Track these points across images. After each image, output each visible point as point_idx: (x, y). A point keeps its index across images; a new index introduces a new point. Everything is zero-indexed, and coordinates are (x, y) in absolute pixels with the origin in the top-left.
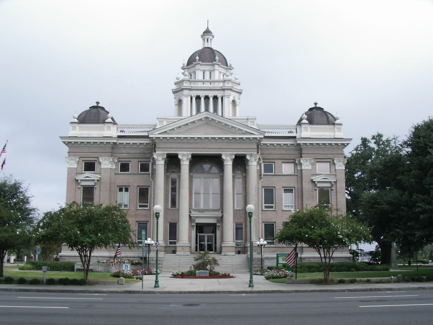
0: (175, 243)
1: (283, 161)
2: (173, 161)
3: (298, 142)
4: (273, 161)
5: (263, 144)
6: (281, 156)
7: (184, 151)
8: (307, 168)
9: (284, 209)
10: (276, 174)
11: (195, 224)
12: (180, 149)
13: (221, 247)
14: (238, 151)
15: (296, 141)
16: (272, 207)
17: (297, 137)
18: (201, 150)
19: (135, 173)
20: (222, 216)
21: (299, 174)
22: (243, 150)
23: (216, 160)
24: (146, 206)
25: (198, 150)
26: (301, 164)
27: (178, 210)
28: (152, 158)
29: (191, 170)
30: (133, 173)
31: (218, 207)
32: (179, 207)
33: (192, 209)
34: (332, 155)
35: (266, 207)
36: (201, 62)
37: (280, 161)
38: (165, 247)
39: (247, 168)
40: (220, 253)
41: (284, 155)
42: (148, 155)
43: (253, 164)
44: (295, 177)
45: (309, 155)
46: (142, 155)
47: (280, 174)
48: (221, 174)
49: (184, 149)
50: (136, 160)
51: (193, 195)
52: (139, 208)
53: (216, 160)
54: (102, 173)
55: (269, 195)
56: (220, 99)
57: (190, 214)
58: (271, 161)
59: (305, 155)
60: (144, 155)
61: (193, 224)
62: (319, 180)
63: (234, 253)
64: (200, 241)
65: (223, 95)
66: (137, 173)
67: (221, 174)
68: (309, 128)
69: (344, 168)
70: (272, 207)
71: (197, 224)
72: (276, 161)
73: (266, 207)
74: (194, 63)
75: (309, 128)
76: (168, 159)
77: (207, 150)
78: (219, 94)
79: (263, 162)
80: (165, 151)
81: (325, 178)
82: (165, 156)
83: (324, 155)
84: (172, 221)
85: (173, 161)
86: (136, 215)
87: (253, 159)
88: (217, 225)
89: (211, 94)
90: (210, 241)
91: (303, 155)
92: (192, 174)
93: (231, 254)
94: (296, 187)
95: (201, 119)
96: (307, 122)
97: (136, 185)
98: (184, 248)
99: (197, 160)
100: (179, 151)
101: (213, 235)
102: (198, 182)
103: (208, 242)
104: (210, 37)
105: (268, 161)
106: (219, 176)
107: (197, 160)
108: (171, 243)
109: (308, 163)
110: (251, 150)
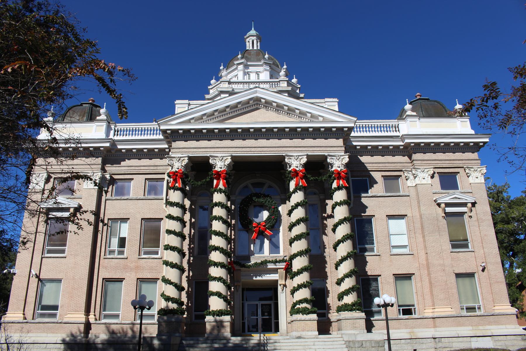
30: (135, 197)
34: (460, 162)
41: (383, 165)
59: (419, 162)
60: (155, 168)
62: (447, 200)
63: (317, 333)
66: (142, 197)
74: (236, 62)
76: (194, 173)
79: (352, 177)
81: (456, 198)
83: (448, 162)
88: (279, 283)
93: (310, 333)
96: (415, 114)
101: (272, 303)
103: (263, 315)
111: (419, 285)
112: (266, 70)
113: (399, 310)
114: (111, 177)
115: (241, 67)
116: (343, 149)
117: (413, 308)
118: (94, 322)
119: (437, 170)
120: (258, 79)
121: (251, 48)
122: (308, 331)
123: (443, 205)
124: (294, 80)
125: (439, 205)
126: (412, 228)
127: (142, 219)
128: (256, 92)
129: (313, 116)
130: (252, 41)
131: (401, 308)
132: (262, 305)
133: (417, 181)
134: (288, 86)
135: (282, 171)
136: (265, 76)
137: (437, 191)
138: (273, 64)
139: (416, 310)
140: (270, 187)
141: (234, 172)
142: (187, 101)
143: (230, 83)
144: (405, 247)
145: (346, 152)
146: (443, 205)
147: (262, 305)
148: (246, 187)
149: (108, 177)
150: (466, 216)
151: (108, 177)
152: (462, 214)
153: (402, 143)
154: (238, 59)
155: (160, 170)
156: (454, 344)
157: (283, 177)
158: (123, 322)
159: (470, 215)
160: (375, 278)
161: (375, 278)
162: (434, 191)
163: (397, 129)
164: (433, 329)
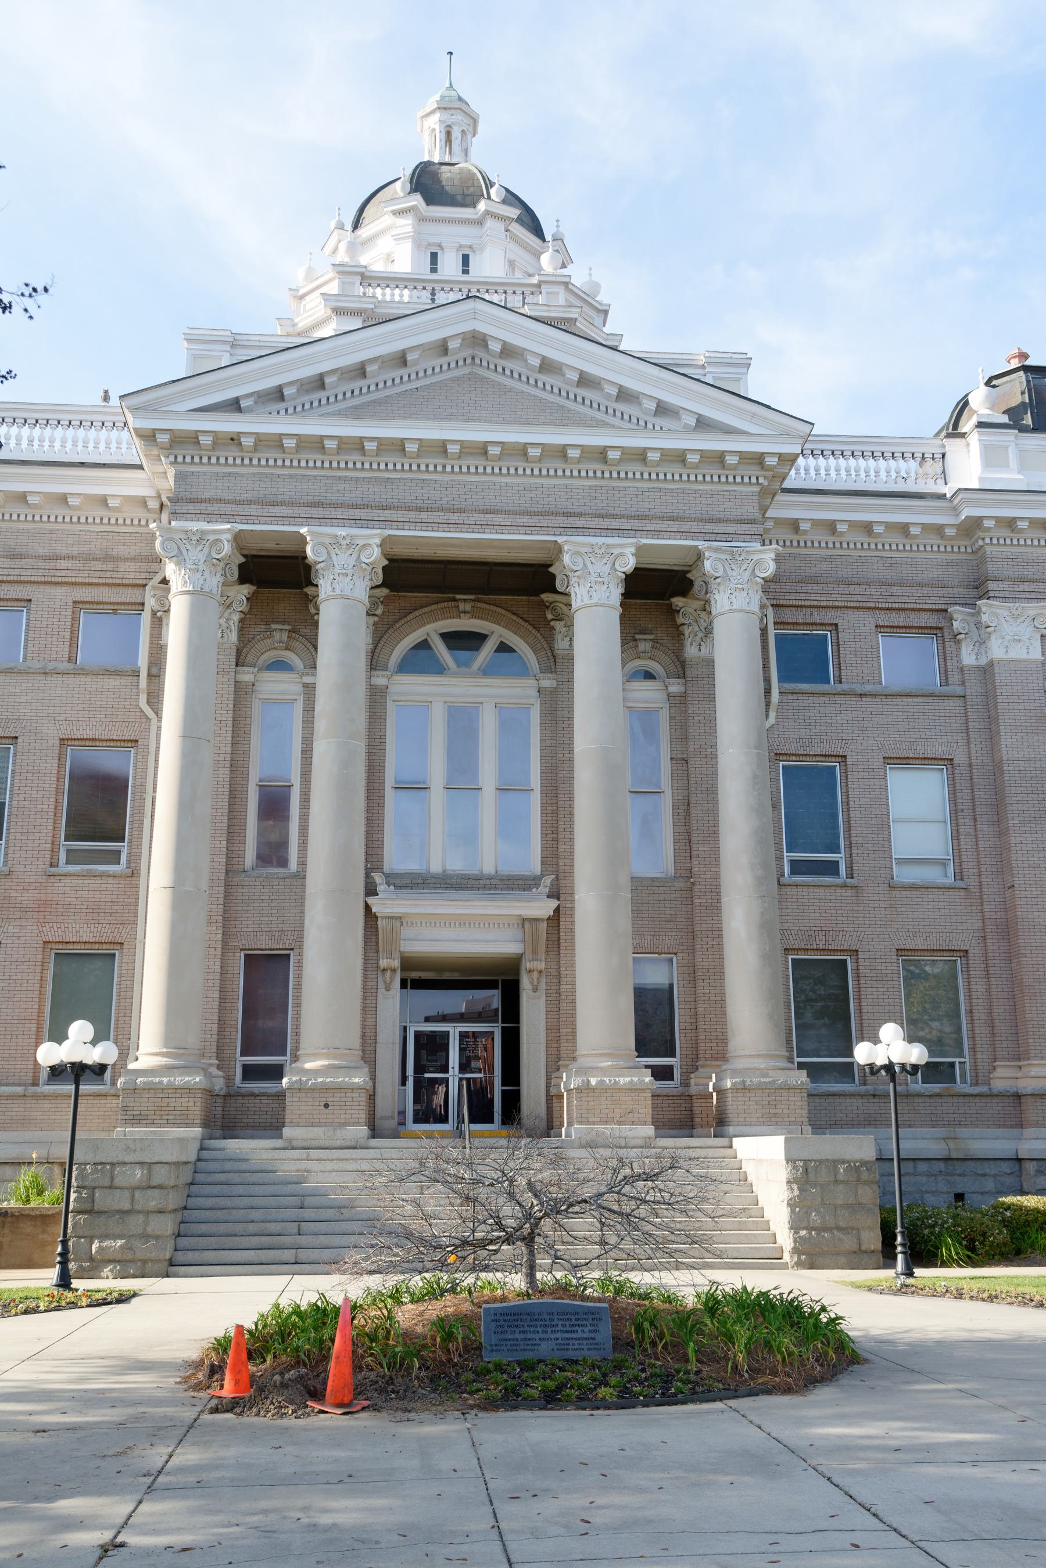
0: (275, 1073)
1: (884, 619)
2: (275, 579)
3: (966, 512)
4: (829, 617)
5: (779, 522)
6: (873, 590)
7: (344, 521)
8: (1017, 653)
9: (903, 875)
10: (845, 687)
11: (396, 964)
13: (552, 1099)
14: (657, 533)
15: (955, 511)
16: (831, 868)
18: (440, 517)
19: (50, 666)
20: (557, 910)
21: (973, 688)
22: (685, 527)
23: (527, 588)
24: (114, 857)
25: (424, 516)
26: (982, 633)
27: (300, 876)
28: (158, 578)
29: (375, 662)
31: (530, 859)
32: (303, 863)
33: (379, 868)
35: (797, 868)
36: (417, 200)
37: (867, 621)
38: (210, 1094)
39: (691, 651)
40: (550, 1127)
42: (132, 566)
43: (740, 600)
44: (953, 706)
45: (1026, 587)
46: (99, 565)
47: (868, 688)
48: (547, 683)
49: (340, 513)
50: (59, 592)
51: (389, 794)
52: (64, 868)
53: (527, 588)
55: (813, 807)
57: (371, 900)
58: (817, 618)
59: (1006, 586)
60: (110, 567)
61: (383, 963)
63: (649, 1130)
64: (419, 1069)
66: (64, 666)
67: (547, 683)
70: (831, 868)
72: (844, 619)
73: (797, 868)
76: (246, 589)
77: (477, 517)
80: (224, 517)
82: (227, 548)
84: (265, 944)
85: (275, 579)
87: (739, 575)
88: (527, 964)
91: (991, 586)
92: (380, 680)
94: (960, 759)
95: (443, 348)
97: (52, 733)
99: (412, 581)
102: (428, 698)
103: (464, 1067)
104: (459, 117)
105: (800, 616)
106: (534, 693)
107: (412, 581)
108: (251, 1073)
109: (1025, 630)
110: (732, 528)
111: (979, 988)
117: (957, 1060)
122: (620, 1123)
126: (964, 802)
129: (663, 409)
132: (463, 1036)
135: (546, 597)
138: (519, 220)
140: (503, 648)
141: (385, 591)
144: (943, 863)
147: (463, 1036)
148: (424, 645)
157: (550, 616)
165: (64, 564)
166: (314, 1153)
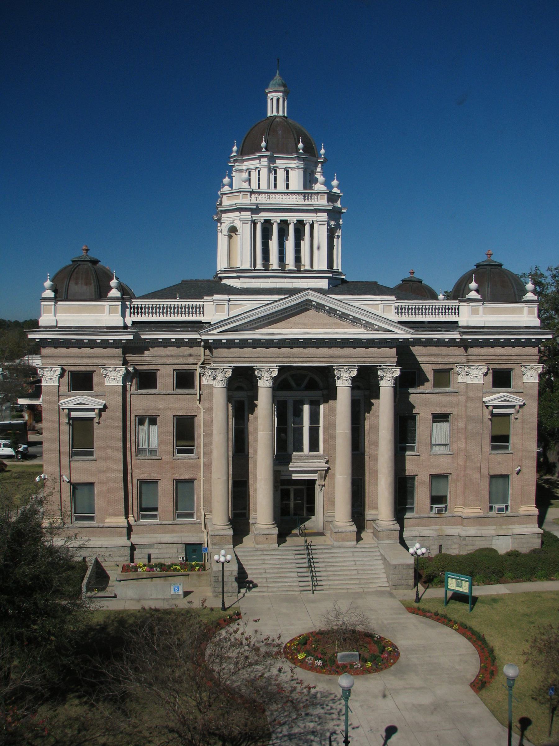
12: (258, 359)
14: (364, 362)
17: (460, 324)
19: (168, 392)
24: (191, 452)
45: (481, 358)
54: (107, 394)
56: (307, 228)
62: (496, 403)
65: (315, 219)
66: (173, 392)
68: (481, 309)
69: (537, 381)
71: (281, 480)
75: (481, 309)
78: (307, 218)
86: (173, 469)
89: (292, 218)
90: (298, 498)
93: (349, 543)
96: (479, 297)
97: (171, 414)
98: (268, 537)
100: (255, 362)
112: (299, 168)
113: (432, 507)
114: (134, 369)
115: (265, 161)
116: (396, 359)
118: (135, 524)
119: (491, 367)
120: (288, 187)
121: (275, 113)
122: (347, 541)
123: (491, 408)
124: (335, 183)
125: (487, 407)
127: (174, 416)
128: (307, 294)
130: (276, 104)
131: (435, 506)
133: (468, 380)
134: (328, 200)
136: (296, 180)
137: (488, 390)
139: (448, 507)
142: (225, 297)
143: (252, 192)
145: (398, 364)
146: (491, 408)
147: (295, 490)
149: (131, 369)
150: (512, 417)
151: (131, 369)
152: (508, 415)
153: (458, 336)
154: (260, 150)
155: (191, 360)
156: (477, 542)
158: (164, 522)
159: (516, 417)
160: (412, 478)
161: (412, 478)
162: (485, 391)
163: (457, 311)
164: (460, 527)
165: (170, 358)
166: (265, 553)
